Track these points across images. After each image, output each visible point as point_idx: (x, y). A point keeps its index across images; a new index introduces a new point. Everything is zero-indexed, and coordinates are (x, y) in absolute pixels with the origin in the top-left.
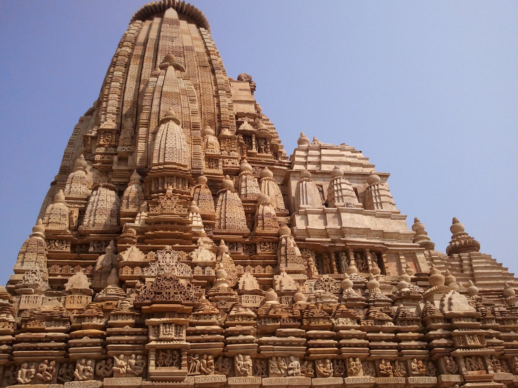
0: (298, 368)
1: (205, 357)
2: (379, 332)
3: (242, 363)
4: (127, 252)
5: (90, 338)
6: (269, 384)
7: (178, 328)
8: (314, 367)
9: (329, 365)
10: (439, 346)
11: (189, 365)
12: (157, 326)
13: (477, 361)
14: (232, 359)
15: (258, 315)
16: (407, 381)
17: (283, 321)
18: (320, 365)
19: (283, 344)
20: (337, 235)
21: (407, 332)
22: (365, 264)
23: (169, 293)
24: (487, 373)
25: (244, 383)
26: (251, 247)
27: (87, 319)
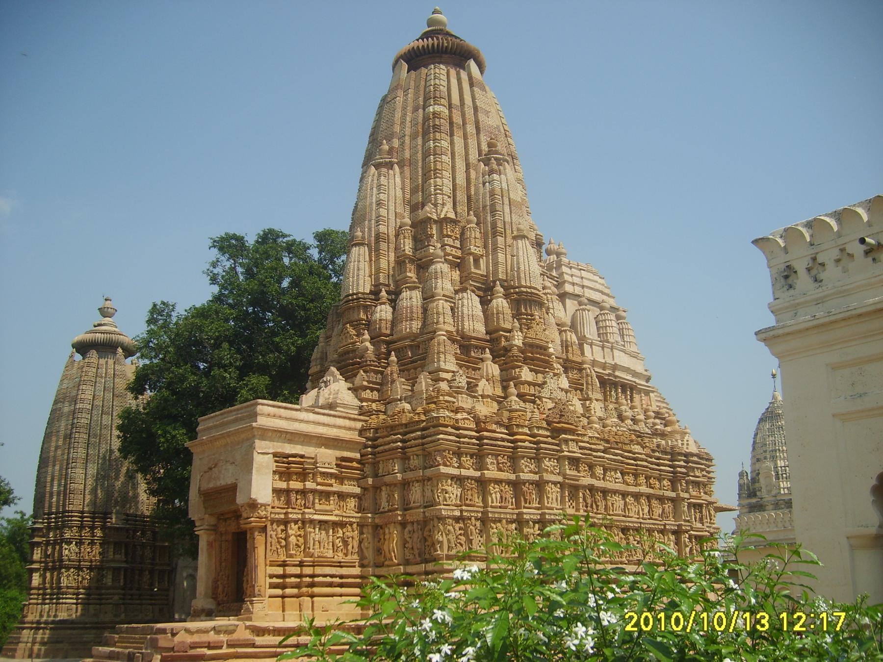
12: (566, 441)
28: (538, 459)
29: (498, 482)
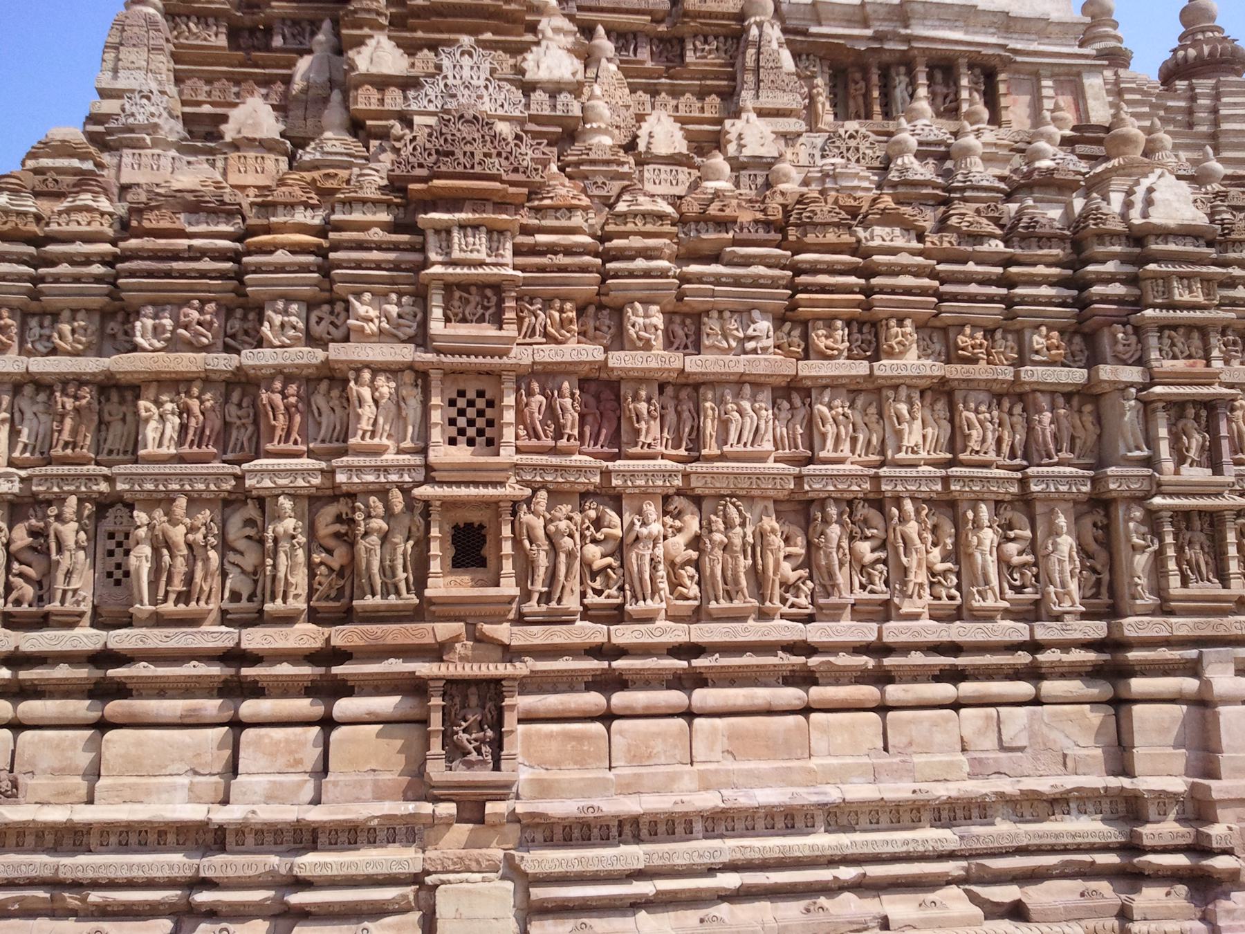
0: (768, 337)
1: (557, 304)
2: (965, 263)
3: (641, 321)
4: (366, 51)
5: (293, 252)
6: (699, 370)
7: (495, 236)
8: (805, 337)
9: (840, 332)
10: (1105, 299)
11: (520, 320)
12: (444, 231)
13: (1188, 337)
14: (618, 312)
15: (682, 214)
16: (1017, 374)
17: (741, 229)
18: (820, 332)
19: (737, 281)
20: (891, 20)
21: (1034, 264)
22: (951, 97)
23: (472, 154)
24: (1208, 365)
25: (645, 365)
26: (670, 48)
27: (280, 209)
28: (327, 305)
29: (177, 383)
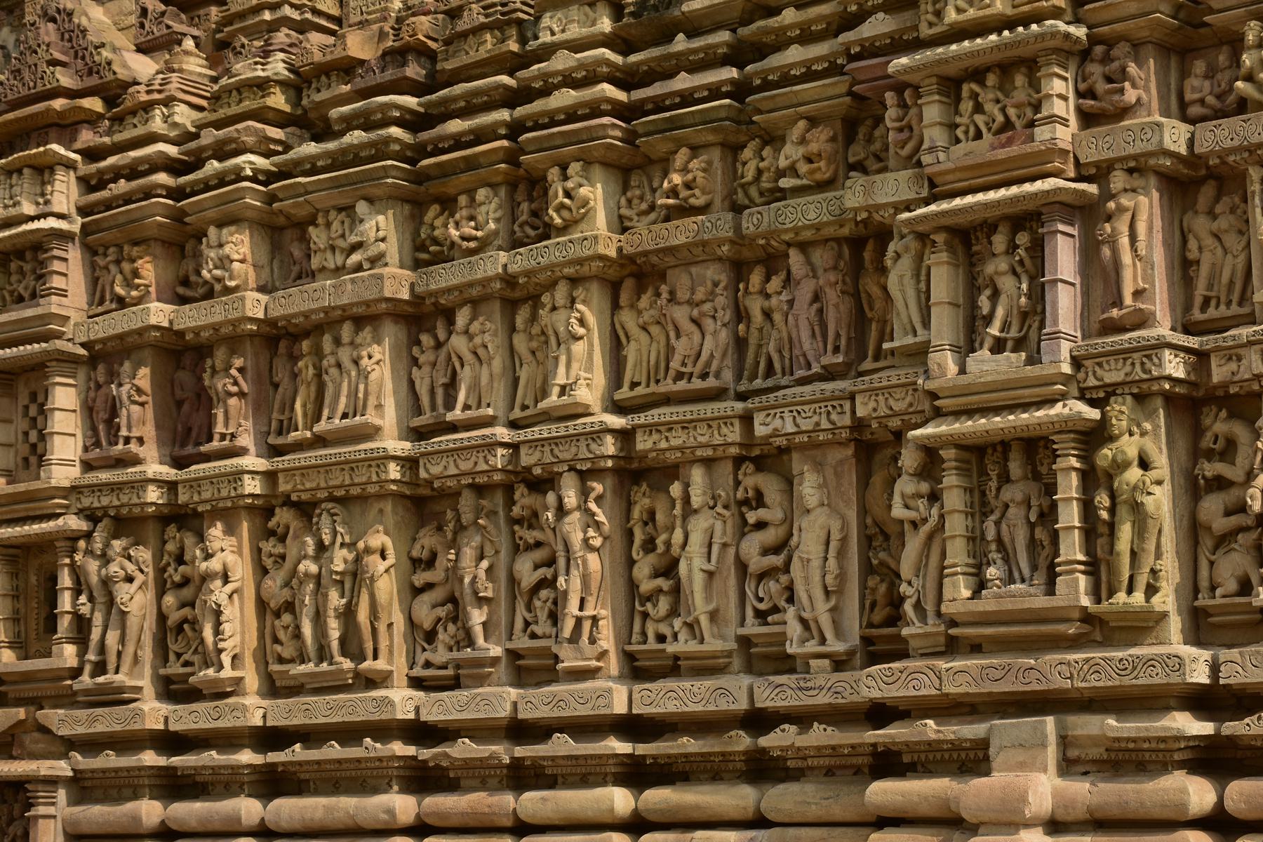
2: (669, 39)
16: (737, 228)
